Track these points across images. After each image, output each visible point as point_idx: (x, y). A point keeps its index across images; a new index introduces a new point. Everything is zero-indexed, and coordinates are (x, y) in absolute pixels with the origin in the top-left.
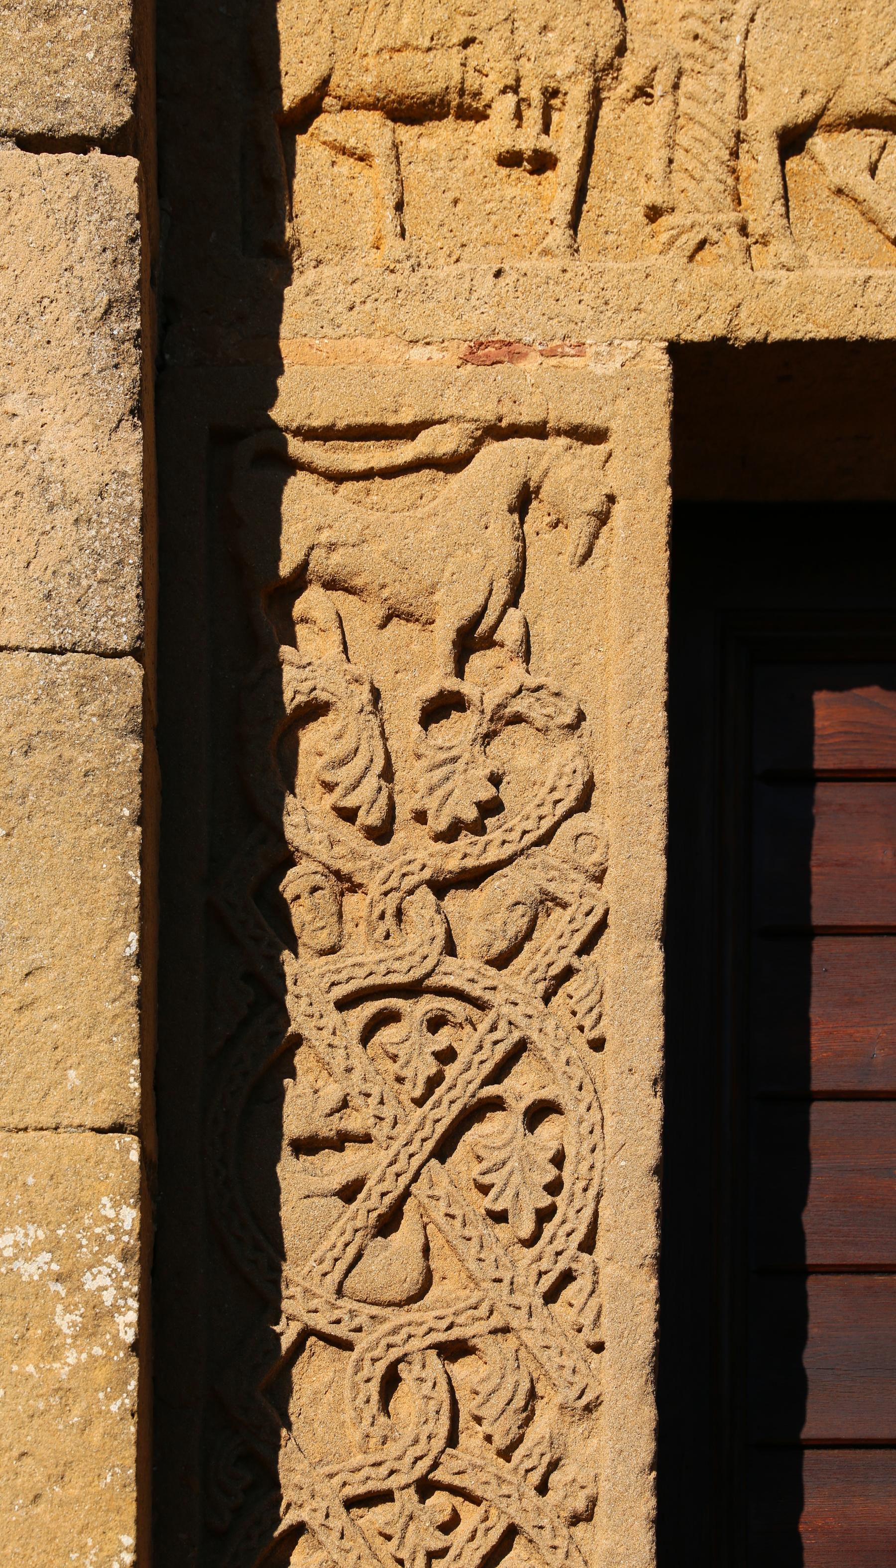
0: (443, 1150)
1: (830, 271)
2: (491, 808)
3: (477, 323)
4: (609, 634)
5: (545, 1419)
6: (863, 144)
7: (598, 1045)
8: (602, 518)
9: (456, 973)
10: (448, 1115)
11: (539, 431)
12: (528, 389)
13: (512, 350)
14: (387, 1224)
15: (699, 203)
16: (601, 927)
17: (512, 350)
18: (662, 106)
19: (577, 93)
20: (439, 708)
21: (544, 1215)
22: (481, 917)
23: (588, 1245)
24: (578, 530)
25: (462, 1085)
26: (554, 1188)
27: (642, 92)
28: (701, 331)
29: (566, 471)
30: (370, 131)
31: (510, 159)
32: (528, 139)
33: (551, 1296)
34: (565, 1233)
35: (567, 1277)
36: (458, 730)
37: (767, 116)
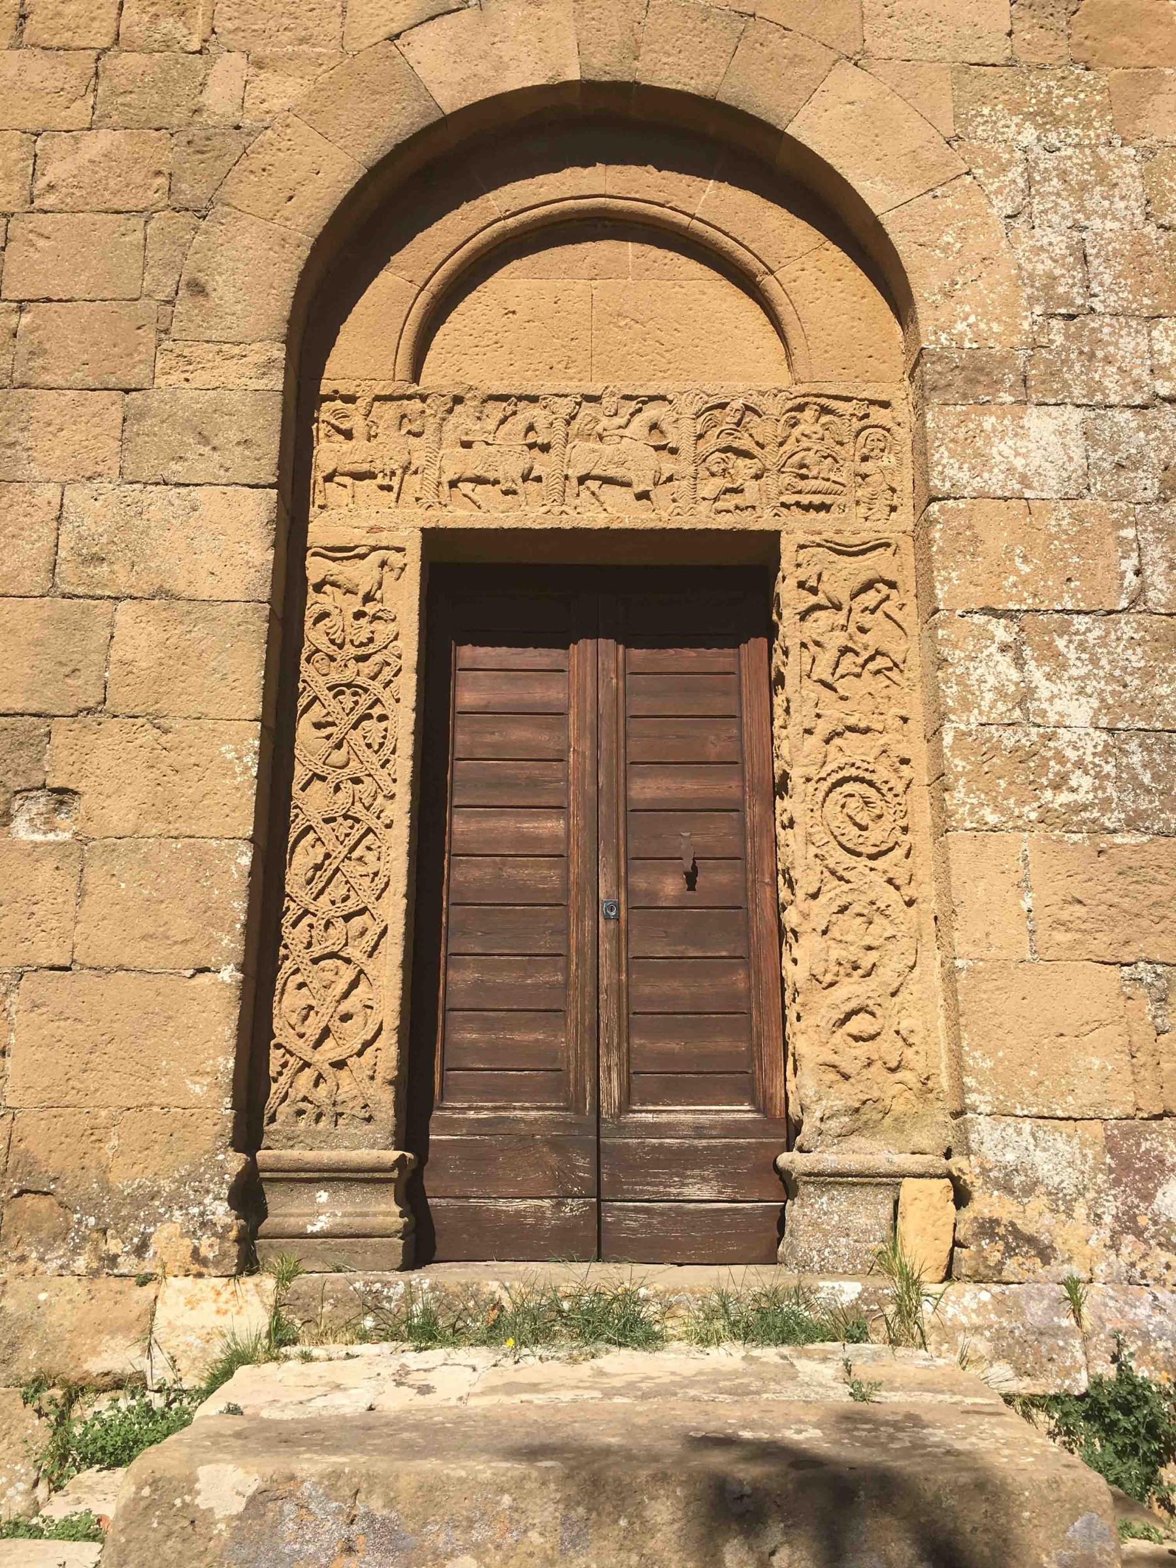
0: (355, 727)
1: (461, 513)
2: (371, 640)
3: (372, 523)
4: (404, 599)
5: (380, 799)
6: (471, 485)
7: (398, 701)
8: (403, 569)
9: (360, 681)
10: (356, 718)
11: (387, 548)
12: (384, 539)
13: (381, 530)
14: (339, 746)
15: (429, 497)
16: (400, 670)
17: (381, 530)
18: (419, 476)
19: (399, 472)
20: (359, 615)
21: (381, 745)
22: (367, 668)
23: (393, 752)
24: (397, 571)
25: (360, 710)
26: (384, 737)
27: (416, 472)
28: (428, 526)
29: (394, 558)
30: (347, 480)
31: (382, 488)
32: (386, 482)
33: (383, 766)
34: (386, 750)
35: (388, 761)
36: (363, 621)
37: (445, 479)
